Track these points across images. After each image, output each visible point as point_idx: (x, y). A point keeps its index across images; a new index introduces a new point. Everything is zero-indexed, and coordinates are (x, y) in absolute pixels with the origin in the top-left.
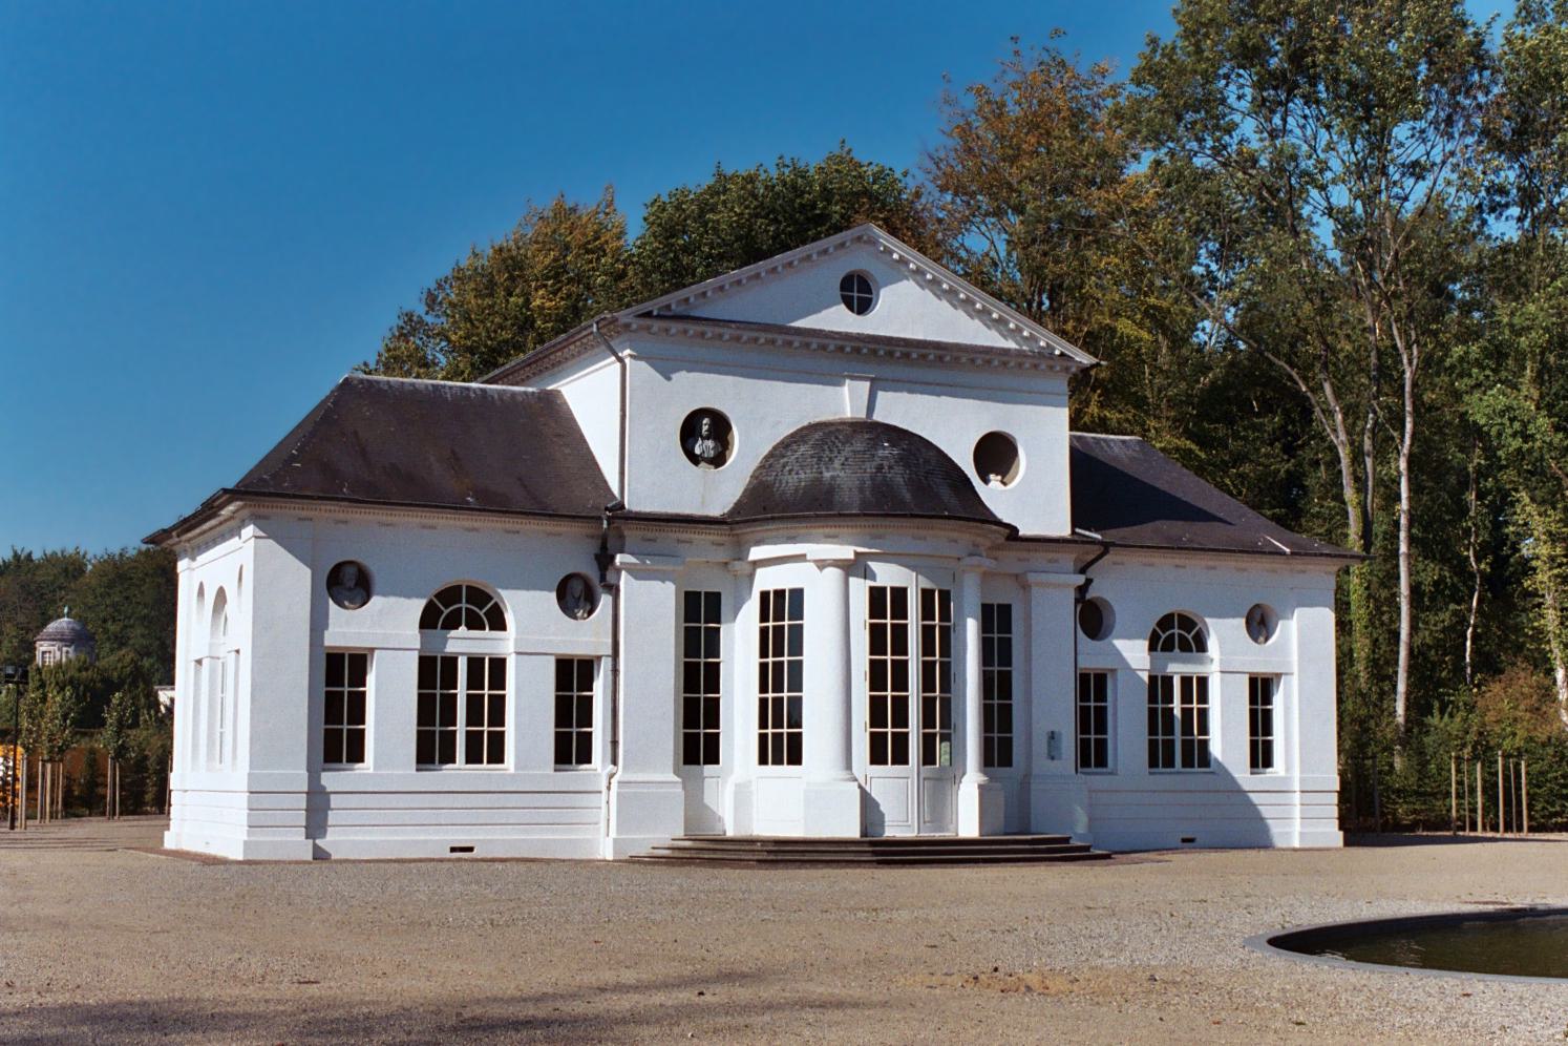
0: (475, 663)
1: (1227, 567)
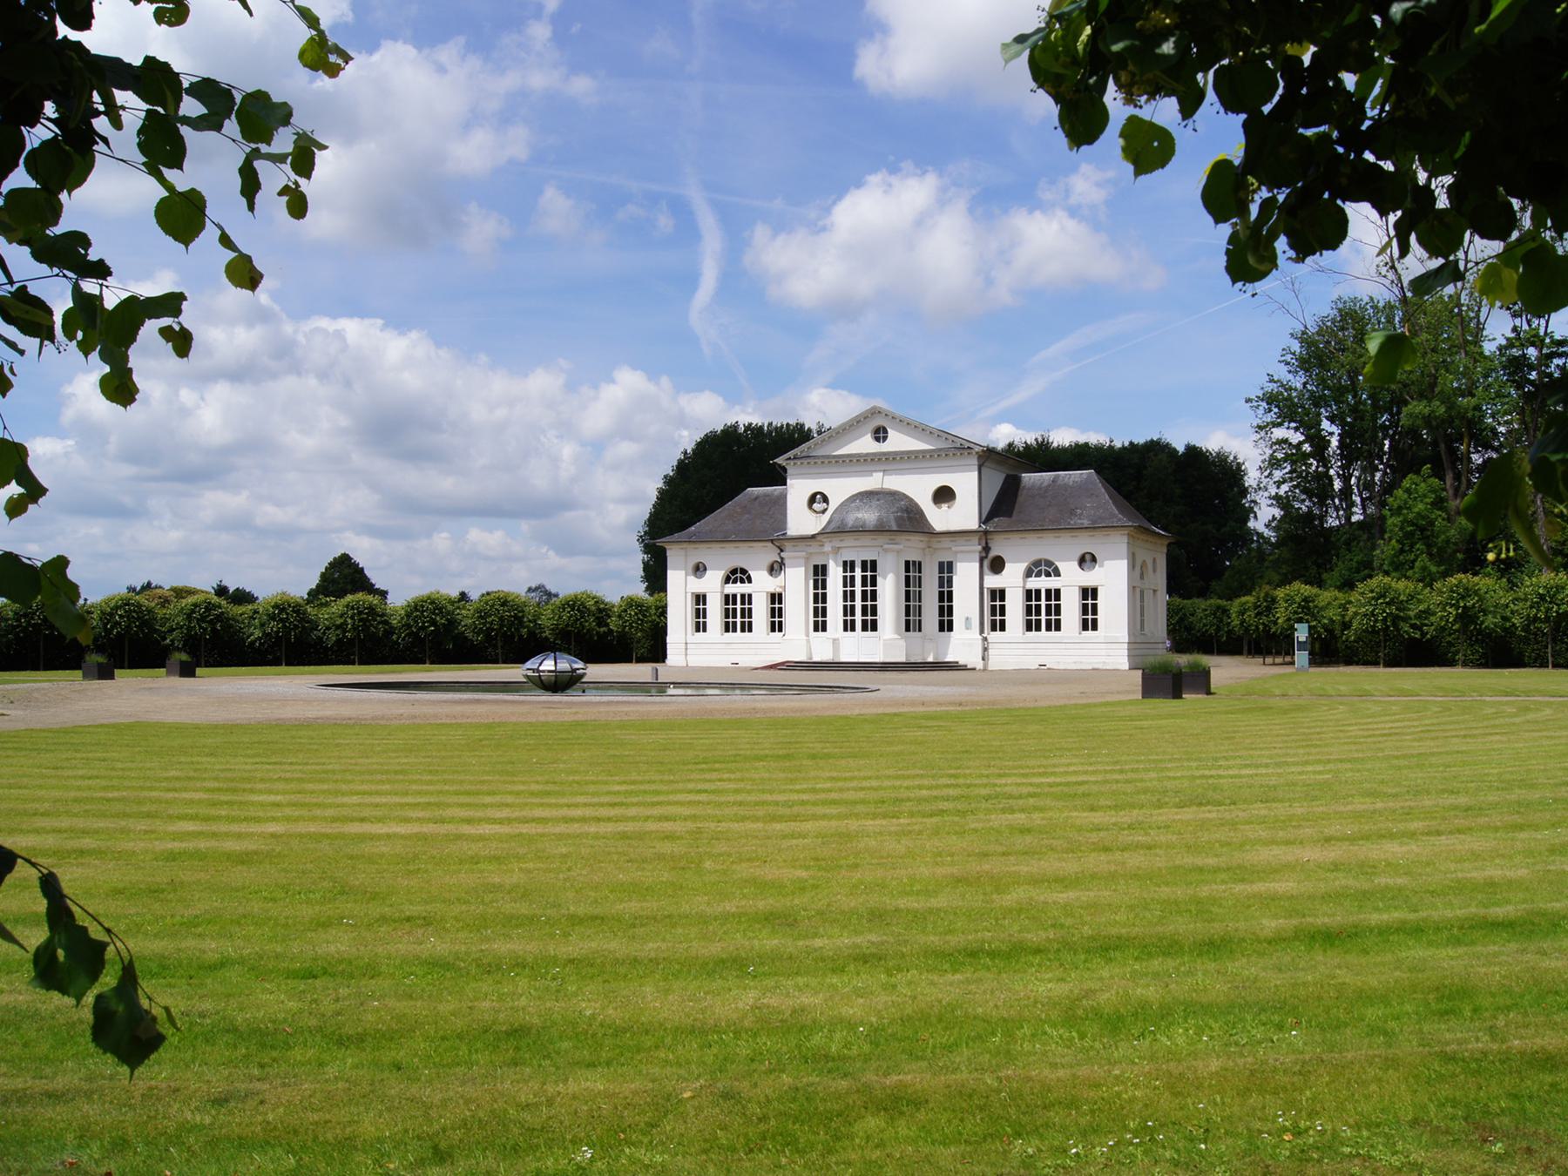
0: (743, 596)
1: (1066, 538)
